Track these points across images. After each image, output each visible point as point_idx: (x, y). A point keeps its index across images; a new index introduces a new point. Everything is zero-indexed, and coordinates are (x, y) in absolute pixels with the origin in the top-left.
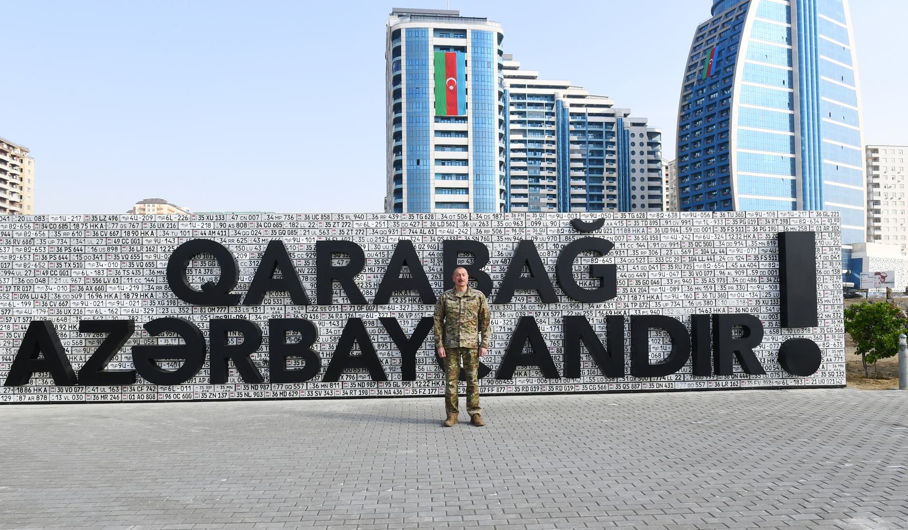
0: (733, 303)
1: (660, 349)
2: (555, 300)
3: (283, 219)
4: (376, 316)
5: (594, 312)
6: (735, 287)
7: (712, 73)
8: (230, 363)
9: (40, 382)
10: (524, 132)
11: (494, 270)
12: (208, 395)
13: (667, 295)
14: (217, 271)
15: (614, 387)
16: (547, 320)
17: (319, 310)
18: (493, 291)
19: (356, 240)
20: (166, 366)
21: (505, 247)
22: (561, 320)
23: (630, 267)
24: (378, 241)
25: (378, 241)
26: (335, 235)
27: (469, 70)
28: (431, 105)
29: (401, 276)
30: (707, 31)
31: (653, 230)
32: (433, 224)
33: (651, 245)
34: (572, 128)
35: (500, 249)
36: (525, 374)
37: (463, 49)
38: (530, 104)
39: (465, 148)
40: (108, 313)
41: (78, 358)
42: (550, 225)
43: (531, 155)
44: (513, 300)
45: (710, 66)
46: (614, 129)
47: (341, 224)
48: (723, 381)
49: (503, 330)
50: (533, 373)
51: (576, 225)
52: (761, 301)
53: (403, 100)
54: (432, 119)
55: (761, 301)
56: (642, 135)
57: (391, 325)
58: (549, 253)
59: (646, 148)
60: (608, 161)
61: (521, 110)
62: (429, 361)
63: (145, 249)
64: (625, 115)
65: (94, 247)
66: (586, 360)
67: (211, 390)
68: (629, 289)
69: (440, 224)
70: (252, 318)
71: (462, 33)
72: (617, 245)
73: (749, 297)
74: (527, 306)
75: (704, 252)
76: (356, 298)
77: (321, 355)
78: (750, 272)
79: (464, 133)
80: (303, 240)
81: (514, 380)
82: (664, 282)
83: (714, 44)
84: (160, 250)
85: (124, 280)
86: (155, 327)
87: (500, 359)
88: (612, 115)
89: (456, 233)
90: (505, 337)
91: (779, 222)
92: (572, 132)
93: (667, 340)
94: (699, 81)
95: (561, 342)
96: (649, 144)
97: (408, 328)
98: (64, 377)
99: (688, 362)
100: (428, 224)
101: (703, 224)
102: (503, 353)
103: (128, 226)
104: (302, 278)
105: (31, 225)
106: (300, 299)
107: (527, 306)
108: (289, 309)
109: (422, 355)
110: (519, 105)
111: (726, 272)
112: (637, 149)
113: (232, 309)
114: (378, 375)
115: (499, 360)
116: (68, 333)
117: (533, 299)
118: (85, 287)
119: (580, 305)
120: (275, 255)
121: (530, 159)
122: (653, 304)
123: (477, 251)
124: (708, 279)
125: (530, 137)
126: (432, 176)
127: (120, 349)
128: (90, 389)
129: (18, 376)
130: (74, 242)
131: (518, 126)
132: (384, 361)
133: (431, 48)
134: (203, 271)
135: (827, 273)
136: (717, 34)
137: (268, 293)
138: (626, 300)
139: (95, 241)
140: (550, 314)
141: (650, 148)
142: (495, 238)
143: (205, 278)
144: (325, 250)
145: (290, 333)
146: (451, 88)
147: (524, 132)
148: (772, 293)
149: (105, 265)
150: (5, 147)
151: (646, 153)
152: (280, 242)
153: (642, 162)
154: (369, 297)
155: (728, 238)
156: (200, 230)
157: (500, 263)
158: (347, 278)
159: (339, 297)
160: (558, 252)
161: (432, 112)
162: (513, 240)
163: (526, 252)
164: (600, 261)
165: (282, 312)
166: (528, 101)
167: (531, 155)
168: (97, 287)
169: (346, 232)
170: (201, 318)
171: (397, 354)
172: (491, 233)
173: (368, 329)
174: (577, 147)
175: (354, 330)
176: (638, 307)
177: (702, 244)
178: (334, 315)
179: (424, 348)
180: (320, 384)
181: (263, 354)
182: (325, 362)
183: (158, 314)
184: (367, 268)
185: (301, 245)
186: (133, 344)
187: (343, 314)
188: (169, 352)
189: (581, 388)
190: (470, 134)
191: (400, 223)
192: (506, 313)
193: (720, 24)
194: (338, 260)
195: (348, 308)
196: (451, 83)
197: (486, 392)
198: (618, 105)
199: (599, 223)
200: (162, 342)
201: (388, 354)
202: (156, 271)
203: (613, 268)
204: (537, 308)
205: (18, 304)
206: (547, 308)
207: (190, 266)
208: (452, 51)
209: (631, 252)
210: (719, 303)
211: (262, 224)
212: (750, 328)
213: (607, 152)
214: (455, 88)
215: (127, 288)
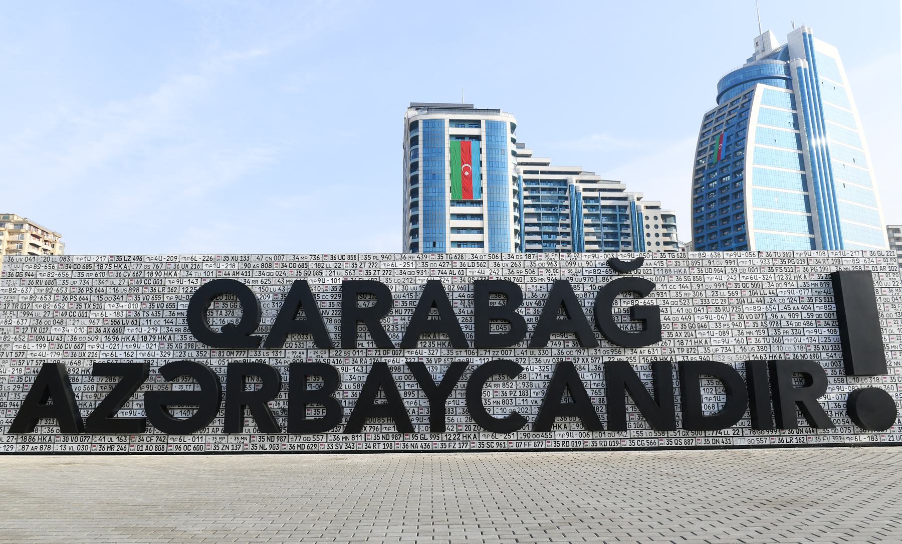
0: (790, 348)
1: (713, 400)
2: (594, 345)
3: (308, 260)
4: (403, 361)
5: (637, 358)
6: (790, 331)
7: (722, 157)
8: (247, 412)
9: (45, 430)
10: (537, 215)
11: (528, 313)
12: (221, 446)
13: (716, 339)
14: (239, 313)
15: (665, 443)
16: (586, 367)
17: (343, 354)
18: (528, 334)
19: (383, 280)
20: (178, 414)
21: (538, 288)
22: (602, 366)
23: (674, 310)
24: (406, 282)
25: (406, 282)
26: (361, 275)
27: (484, 157)
28: (447, 190)
29: (429, 318)
30: (714, 118)
31: (696, 270)
32: (463, 265)
33: (695, 287)
34: (585, 211)
35: (533, 290)
36: (565, 427)
37: (478, 138)
38: (543, 189)
39: (480, 230)
40: (123, 356)
41: (88, 405)
42: (585, 265)
43: (546, 237)
44: (549, 344)
45: (720, 151)
46: (628, 212)
47: (367, 265)
48: (787, 436)
49: (539, 378)
50: (574, 426)
51: (614, 265)
52: (820, 346)
53: (420, 185)
54: (448, 203)
55: (820, 346)
56: (656, 218)
57: (418, 370)
58: (586, 294)
59: (662, 231)
60: (623, 243)
61: (535, 194)
62: (459, 411)
63: (166, 290)
64: (638, 199)
65: (115, 288)
66: (632, 412)
67: (224, 442)
68: (674, 333)
69: (470, 264)
70: (273, 363)
71: (477, 124)
72: (658, 286)
73: (806, 342)
74: (565, 351)
75: (753, 294)
76: (383, 342)
77: (343, 404)
78: (804, 315)
79: (480, 216)
80: (328, 281)
81: (553, 434)
82: (712, 325)
83: (722, 130)
84: (181, 291)
85: (143, 321)
86: (171, 371)
87: (537, 410)
88: (625, 199)
89: (487, 274)
90: (541, 385)
91: (831, 262)
92: (585, 215)
93: (721, 389)
94: (709, 165)
95: (603, 391)
96: (664, 226)
97: (437, 374)
98: (72, 425)
99: (746, 414)
100: (458, 264)
101: (748, 264)
102: (540, 403)
103: (152, 266)
104: (325, 320)
105: (56, 265)
106: (323, 342)
107: (565, 351)
108: (311, 354)
109: (452, 405)
110: (533, 189)
111: (779, 315)
112: (652, 231)
113: (252, 353)
114: (405, 427)
115: (535, 410)
116: (80, 378)
117: (571, 344)
118: (102, 329)
119: (622, 350)
120: (299, 296)
121: (545, 242)
122: (701, 350)
123: (509, 291)
124: (759, 323)
125: (544, 220)
127: (132, 395)
128: (96, 439)
129: (23, 425)
130: (96, 282)
131: (532, 210)
132: (411, 411)
133: (447, 137)
134: (224, 312)
135: (890, 317)
136: (724, 121)
137: (290, 336)
138: (672, 345)
139: (117, 282)
140: (590, 360)
141: (665, 231)
142: (528, 279)
143: (226, 320)
144: (351, 290)
145: (311, 379)
146: (467, 173)
147: (537, 215)
148: (831, 338)
149: (125, 306)
151: (661, 235)
152: (305, 282)
153: (658, 244)
154: (396, 338)
155: (777, 279)
156: (224, 270)
157: (533, 305)
158: (373, 320)
159: (365, 341)
160: (596, 294)
161: (448, 197)
162: (547, 281)
163: (561, 291)
164: (641, 302)
165: (304, 356)
166: (541, 186)
167: (546, 237)
168: (116, 329)
169: (373, 272)
170: (217, 362)
171: (425, 403)
172: (524, 273)
173: (394, 375)
174: (592, 229)
175: (380, 376)
176: (685, 352)
177: (749, 285)
178: (358, 359)
179: (454, 396)
180: (341, 436)
181: (281, 402)
182: (347, 412)
183: (174, 356)
184: (394, 310)
185: (327, 286)
186: (146, 389)
187: (368, 359)
188: (182, 399)
189: (627, 444)
190: (486, 217)
191: (429, 263)
192: (542, 359)
193: (726, 111)
194: (365, 300)
195: (373, 353)
196: (467, 169)
197: (523, 447)
198: (631, 190)
199: (639, 262)
200: (176, 388)
201: (415, 403)
202: (176, 312)
203: (656, 309)
204: (575, 354)
205: (33, 346)
206: (586, 354)
207: (211, 307)
208: (467, 140)
209: (673, 294)
210: (775, 348)
211: (288, 264)
212: (810, 376)
213: (622, 234)
214: (471, 173)
215: (145, 330)
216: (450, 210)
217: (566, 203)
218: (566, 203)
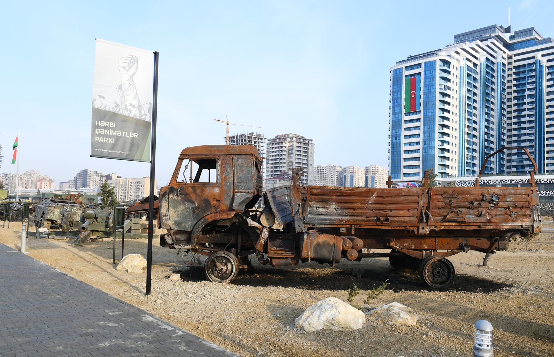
71: (419, 65)
126: (402, 145)
133: (404, 78)
146: (413, 96)
150: (301, 140)
161: (403, 111)
196: (413, 94)
216: (404, 118)
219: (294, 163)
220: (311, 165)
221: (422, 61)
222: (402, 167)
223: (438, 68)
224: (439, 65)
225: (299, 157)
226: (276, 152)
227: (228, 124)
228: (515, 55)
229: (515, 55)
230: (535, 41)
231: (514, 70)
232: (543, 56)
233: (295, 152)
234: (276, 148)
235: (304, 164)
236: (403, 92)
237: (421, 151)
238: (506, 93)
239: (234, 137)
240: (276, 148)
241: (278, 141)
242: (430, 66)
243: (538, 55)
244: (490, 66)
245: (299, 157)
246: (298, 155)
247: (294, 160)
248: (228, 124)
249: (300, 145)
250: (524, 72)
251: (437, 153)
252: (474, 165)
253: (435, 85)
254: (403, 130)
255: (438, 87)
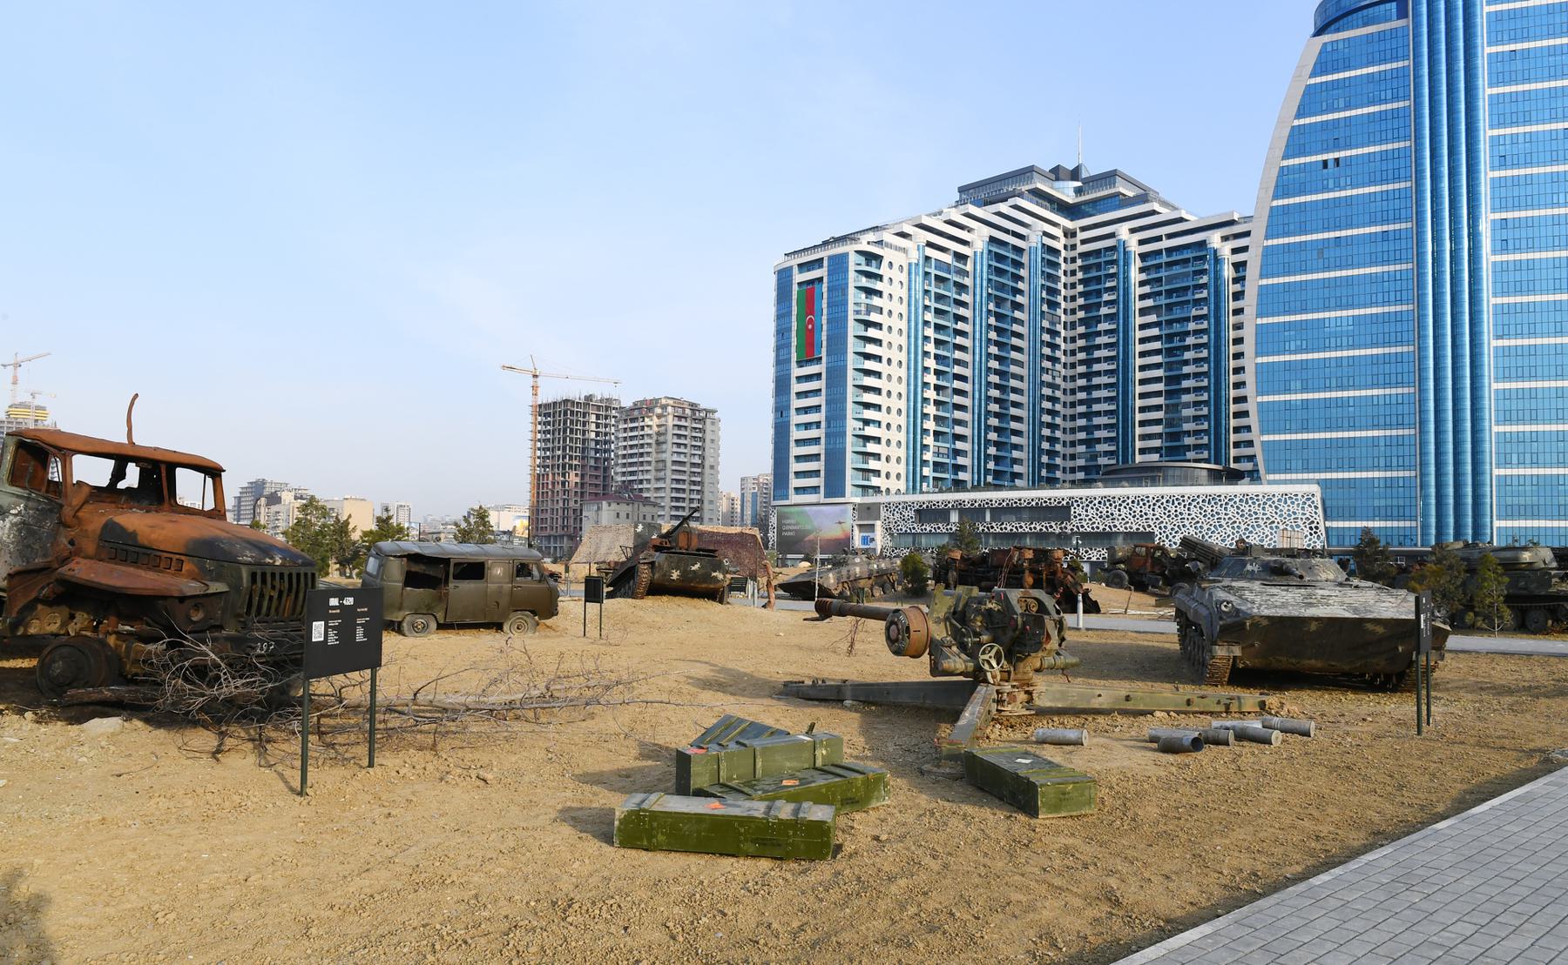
126: (793, 428)
133: (795, 288)
150: (688, 412)
217: (1205, 279)
218: (1205, 279)
219: (669, 464)
220: (712, 467)
221: (823, 254)
222: (792, 475)
223: (852, 268)
224: (854, 262)
225: (682, 450)
226: (632, 438)
227: (535, 376)
228: (1083, 229)
229: (1083, 229)
230: (1120, 201)
231: (1079, 262)
232: (1133, 231)
233: (670, 439)
234: (632, 429)
235: (693, 465)
236: (794, 318)
237: (823, 441)
238: (1060, 312)
239: (547, 406)
240: (632, 429)
241: (636, 413)
242: (839, 263)
243: (1123, 230)
244: (1004, 259)
245: (682, 450)
246: (679, 445)
247: (668, 457)
248: (535, 376)
249: (683, 423)
250: (1098, 266)
251: (851, 444)
252: (958, 468)
253: (845, 303)
254: (793, 396)
255: (851, 307)
